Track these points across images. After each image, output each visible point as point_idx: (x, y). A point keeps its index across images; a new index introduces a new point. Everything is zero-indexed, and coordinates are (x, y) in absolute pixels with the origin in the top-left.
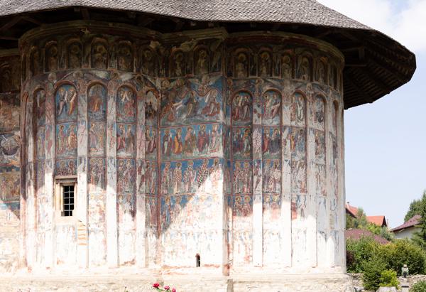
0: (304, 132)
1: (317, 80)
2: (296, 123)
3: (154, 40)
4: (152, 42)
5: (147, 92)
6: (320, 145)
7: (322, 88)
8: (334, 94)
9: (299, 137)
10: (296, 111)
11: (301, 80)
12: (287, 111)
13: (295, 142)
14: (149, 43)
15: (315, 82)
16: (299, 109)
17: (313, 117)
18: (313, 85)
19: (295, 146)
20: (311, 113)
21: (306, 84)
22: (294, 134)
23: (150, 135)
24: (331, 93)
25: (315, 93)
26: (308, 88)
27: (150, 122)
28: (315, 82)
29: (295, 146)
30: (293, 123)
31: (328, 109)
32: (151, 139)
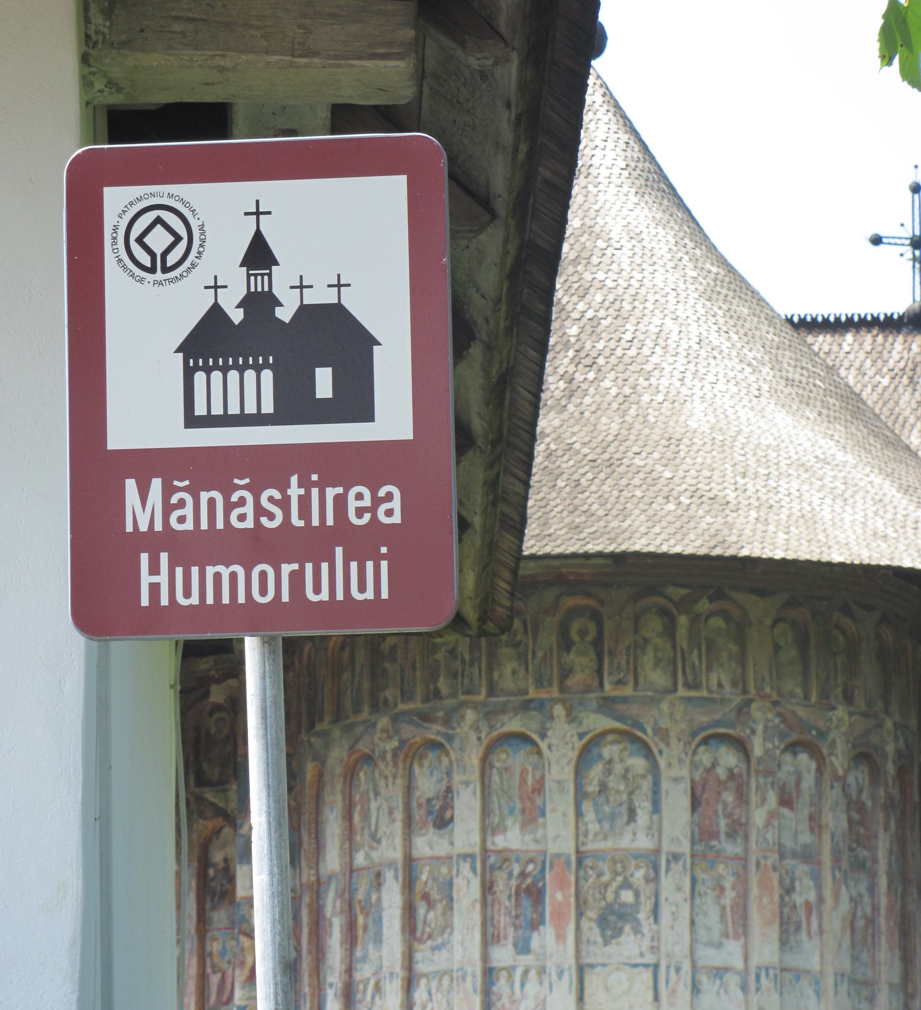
0: (378, 880)
1: (406, 696)
2: (367, 856)
3: (219, 681)
4: (214, 689)
5: (218, 832)
6: (439, 907)
7: (426, 718)
8: (490, 714)
9: (374, 897)
10: (366, 816)
11: (365, 714)
12: (333, 828)
13: (367, 915)
14: (207, 694)
15: (402, 707)
16: (373, 805)
17: (398, 826)
18: (395, 719)
19: (365, 928)
20: (391, 813)
21: (374, 725)
22: (360, 895)
23: (223, 953)
24: (470, 715)
25: (402, 742)
26: (382, 739)
27: (219, 917)
28: (402, 707)
29: (365, 928)
30: (360, 859)
31: (457, 778)
32: (224, 965)
